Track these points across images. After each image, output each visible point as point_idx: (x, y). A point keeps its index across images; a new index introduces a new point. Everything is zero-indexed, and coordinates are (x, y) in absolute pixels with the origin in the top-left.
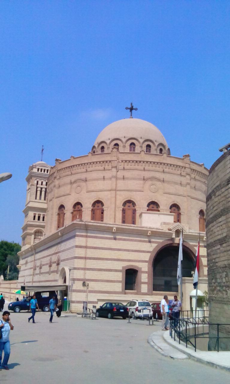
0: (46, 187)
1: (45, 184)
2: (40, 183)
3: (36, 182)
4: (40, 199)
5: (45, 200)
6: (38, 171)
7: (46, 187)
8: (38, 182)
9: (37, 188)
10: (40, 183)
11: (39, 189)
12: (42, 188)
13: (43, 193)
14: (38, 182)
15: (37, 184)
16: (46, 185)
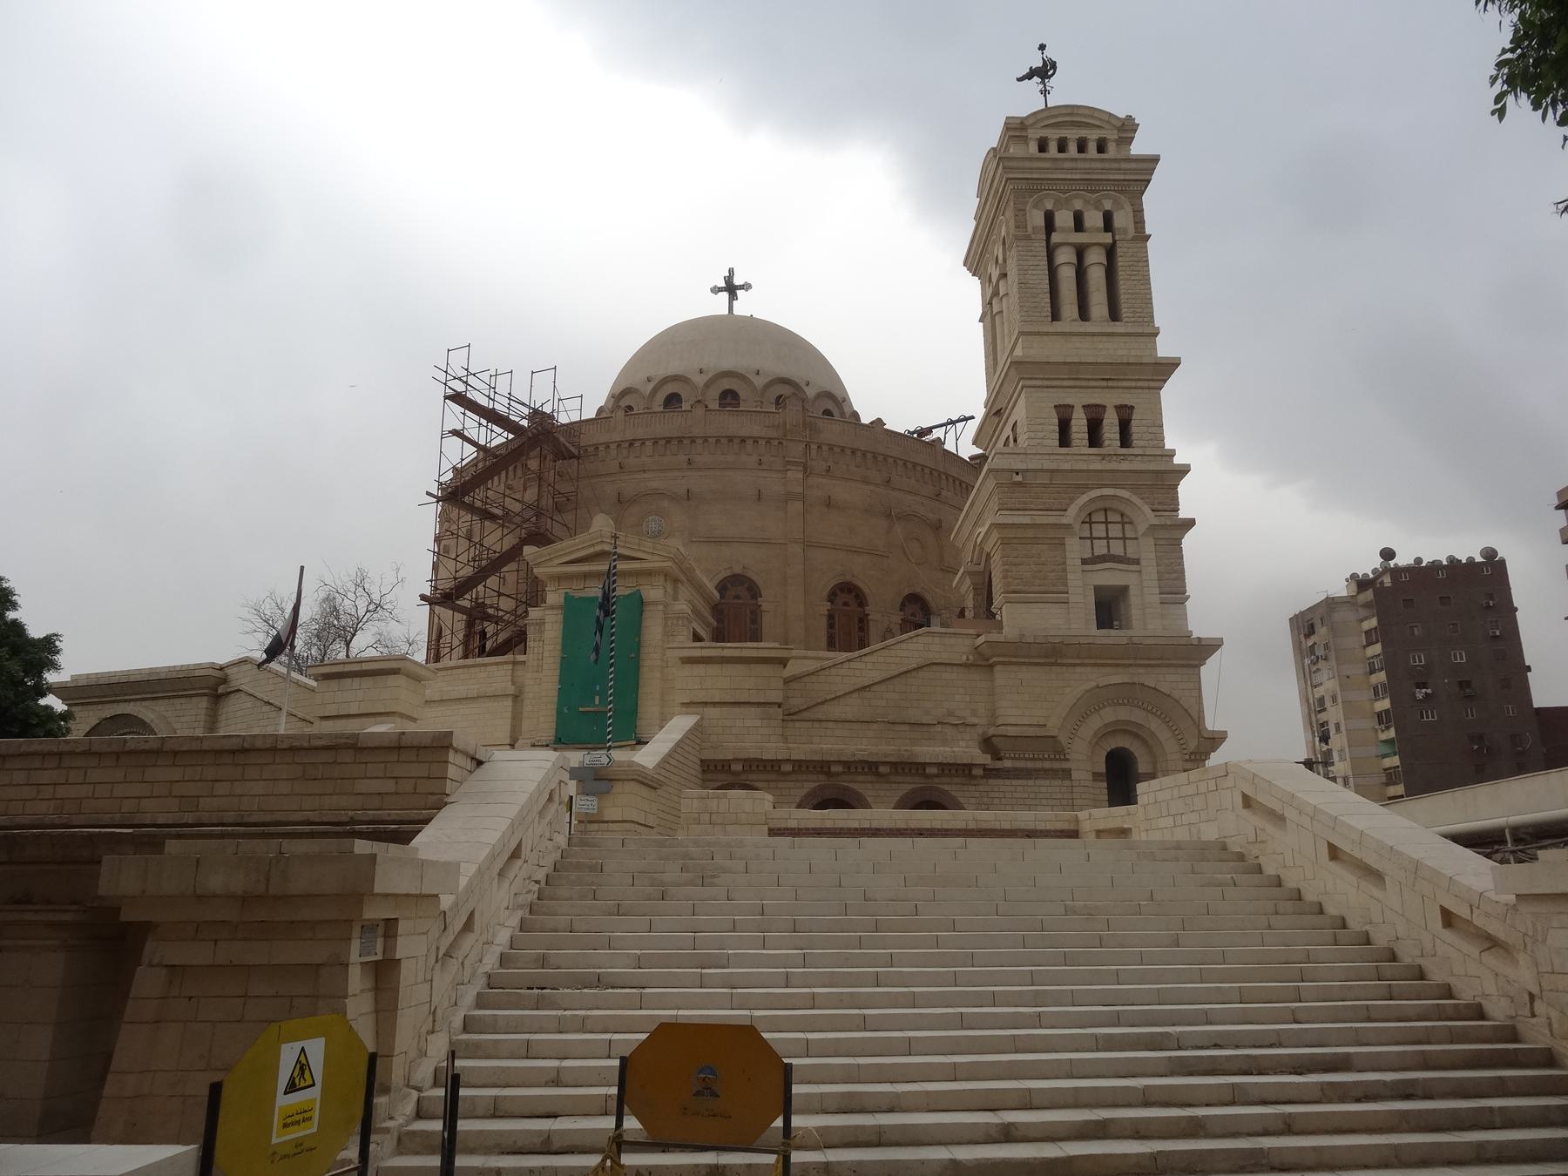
0: (1107, 238)
1: (1101, 224)
2: (1064, 219)
3: (1038, 219)
4: (1084, 314)
5: (1114, 315)
6: (1043, 148)
7: (1107, 238)
8: (1049, 218)
9: (1050, 253)
10: (1064, 219)
11: (1065, 257)
12: (1080, 251)
13: (1096, 276)
14: (1049, 218)
15: (1050, 226)
16: (1108, 225)
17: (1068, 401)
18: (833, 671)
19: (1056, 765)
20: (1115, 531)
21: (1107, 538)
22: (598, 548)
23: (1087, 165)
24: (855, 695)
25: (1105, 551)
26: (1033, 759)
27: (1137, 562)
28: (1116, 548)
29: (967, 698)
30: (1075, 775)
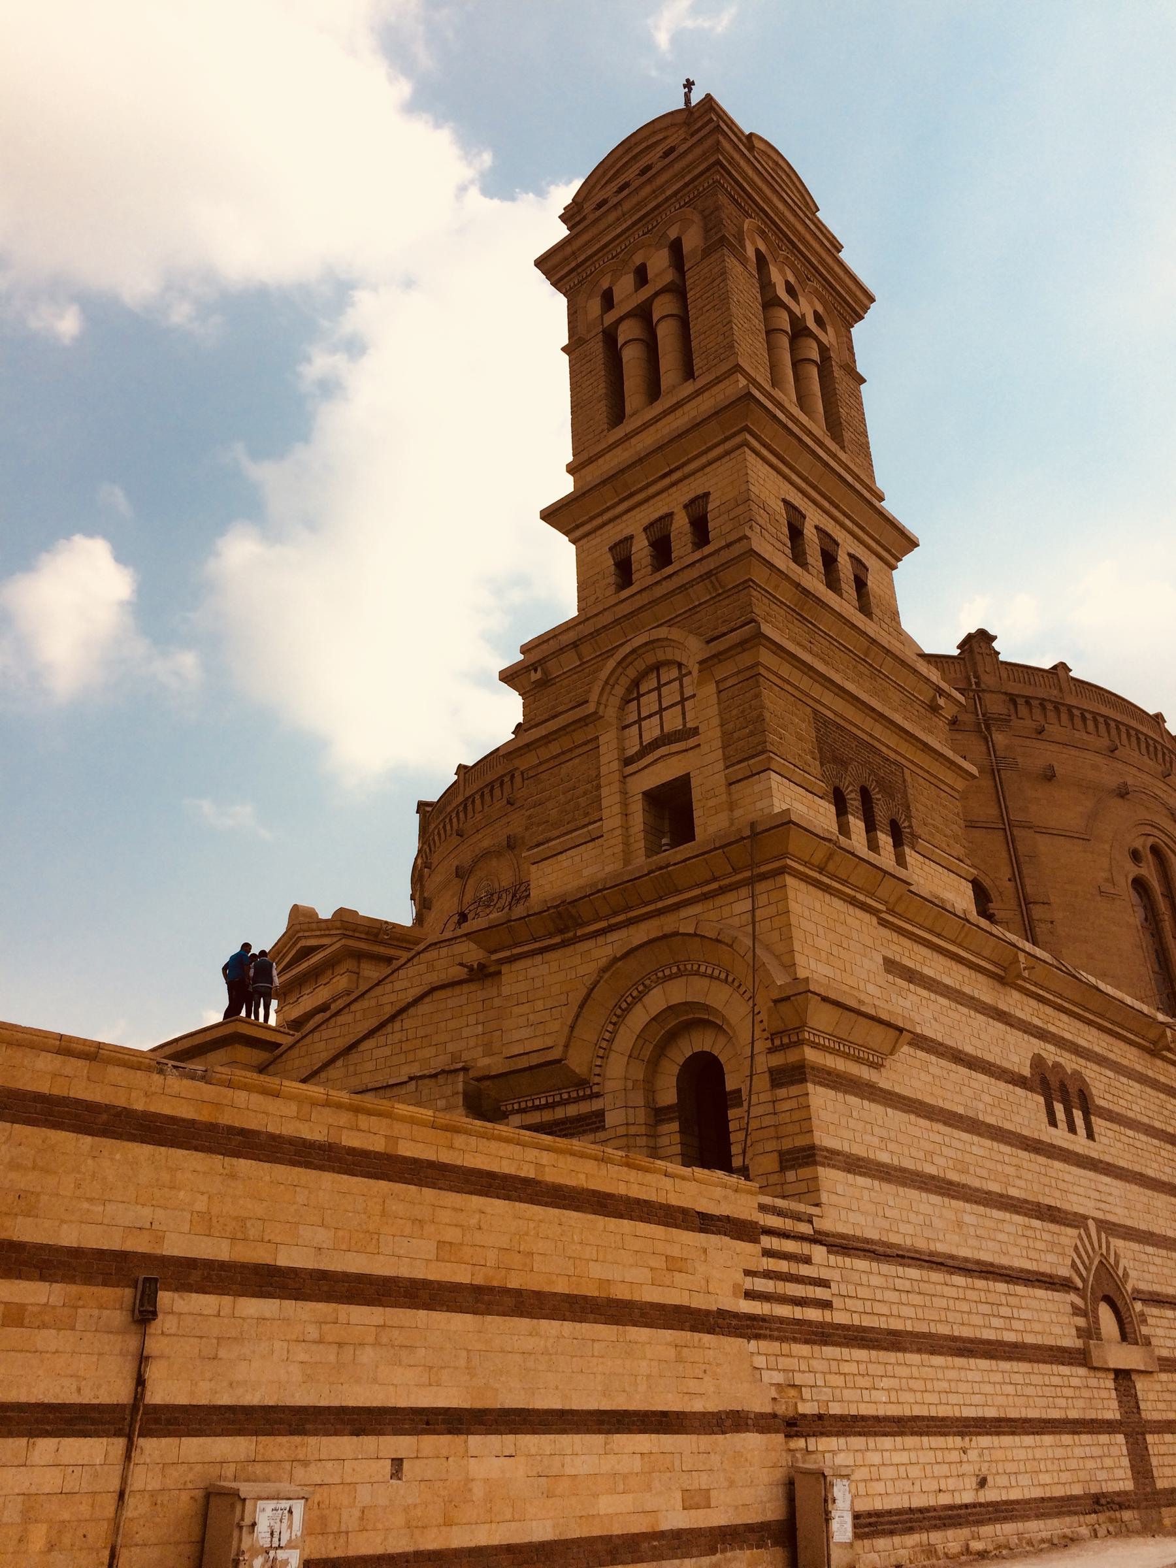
5: (689, 373)
12: (643, 313)
17: (626, 533)
18: (316, 1035)
19: (585, 1108)
20: (670, 694)
21: (661, 710)
22: (298, 946)
23: (635, 200)
24: (339, 1063)
25: (656, 733)
26: (547, 1106)
27: (695, 731)
28: (673, 721)
29: (480, 1028)
30: (611, 1119)
